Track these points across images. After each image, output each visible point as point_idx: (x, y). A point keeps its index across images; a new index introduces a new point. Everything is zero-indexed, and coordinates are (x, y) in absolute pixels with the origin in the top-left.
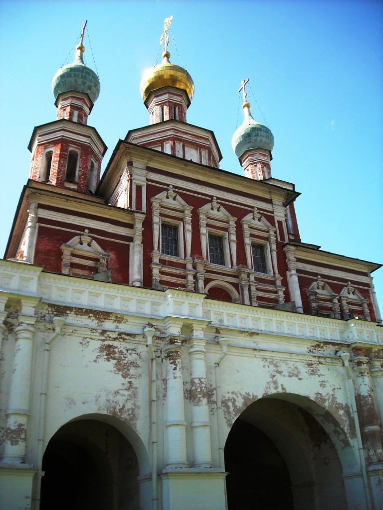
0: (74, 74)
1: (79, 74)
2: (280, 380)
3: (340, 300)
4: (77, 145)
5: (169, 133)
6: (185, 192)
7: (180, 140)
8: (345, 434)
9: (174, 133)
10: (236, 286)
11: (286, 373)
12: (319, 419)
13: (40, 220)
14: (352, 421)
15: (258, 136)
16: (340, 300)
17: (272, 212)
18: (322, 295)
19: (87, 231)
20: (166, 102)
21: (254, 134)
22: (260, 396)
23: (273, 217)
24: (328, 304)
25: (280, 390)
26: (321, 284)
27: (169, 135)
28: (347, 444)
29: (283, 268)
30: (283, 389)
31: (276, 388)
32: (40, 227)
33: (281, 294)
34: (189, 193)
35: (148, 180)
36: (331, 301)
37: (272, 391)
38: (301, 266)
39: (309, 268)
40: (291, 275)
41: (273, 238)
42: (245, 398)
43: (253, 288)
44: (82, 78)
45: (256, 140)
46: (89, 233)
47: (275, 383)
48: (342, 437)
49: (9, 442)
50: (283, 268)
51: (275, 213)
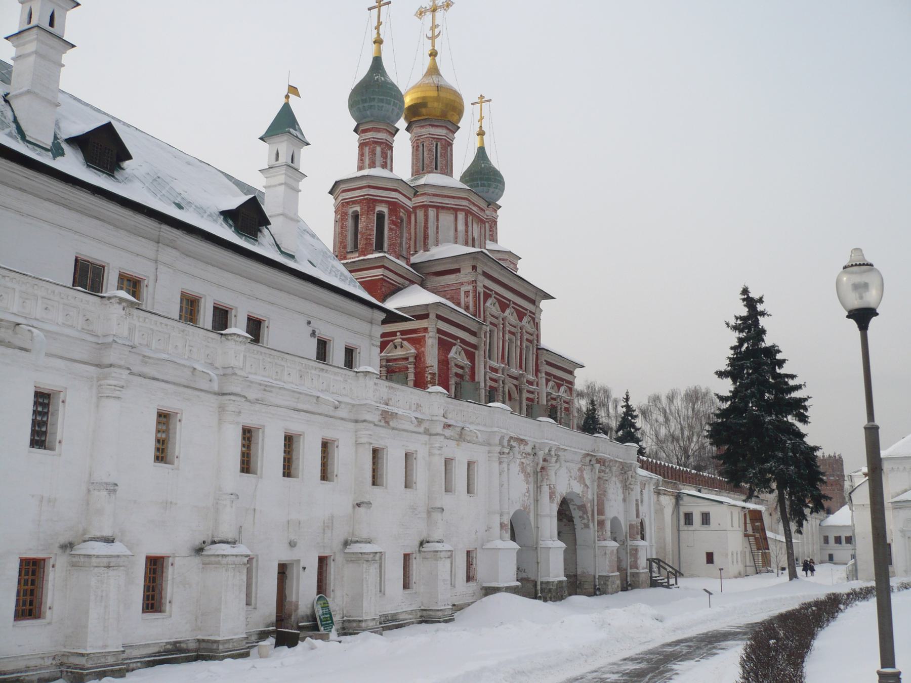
0: (394, 102)
1: (397, 103)
4: (404, 210)
5: (465, 203)
6: (500, 298)
7: (471, 213)
8: (589, 520)
9: (468, 205)
10: (516, 386)
13: (439, 331)
14: (593, 511)
15: (497, 188)
19: (459, 340)
20: (441, 139)
21: (494, 186)
27: (464, 206)
28: (587, 526)
29: (537, 371)
32: (439, 338)
34: (505, 301)
35: (485, 287)
37: (569, 491)
40: (541, 378)
42: (560, 496)
44: (398, 109)
45: (493, 192)
46: (460, 342)
48: (585, 521)
49: (505, 532)
50: (537, 371)
51: (536, 315)
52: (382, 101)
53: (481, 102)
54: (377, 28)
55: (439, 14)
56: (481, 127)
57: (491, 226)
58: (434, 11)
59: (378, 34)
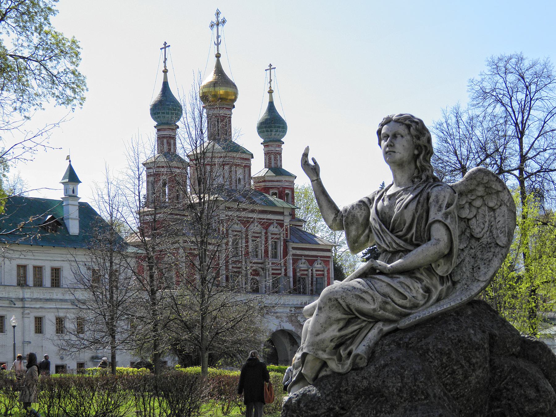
2: (282, 324)
3: (312, 270)
10: (263, 269)
11: (285, 321)
12: (295, 337)
16: (312, 270)
17: (283, 221)
18: (303, 267)
22: (275, 331)
23: (283, 223)
24: (306, 273)
25: (282, 328)
26: (303, 261)
29: (285, 253)
30: (283, 327)
31: (281, 327)
33: (283, 270)
36: (307, 270)
37: (279, 329)
38: (294, 252)
39: (298, 252)
41: (282, 238)
43: (270, 269)
45: (275, 135)
47: (280, 325)
50: (285, 253)
52: (164, 113)
53: (270, 69)
54: (165, 62)
55: (220, 27)
56: (270, 87)
57: (275, 157)
58: (218, 25)
59: (165, 66)
